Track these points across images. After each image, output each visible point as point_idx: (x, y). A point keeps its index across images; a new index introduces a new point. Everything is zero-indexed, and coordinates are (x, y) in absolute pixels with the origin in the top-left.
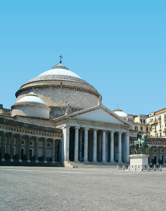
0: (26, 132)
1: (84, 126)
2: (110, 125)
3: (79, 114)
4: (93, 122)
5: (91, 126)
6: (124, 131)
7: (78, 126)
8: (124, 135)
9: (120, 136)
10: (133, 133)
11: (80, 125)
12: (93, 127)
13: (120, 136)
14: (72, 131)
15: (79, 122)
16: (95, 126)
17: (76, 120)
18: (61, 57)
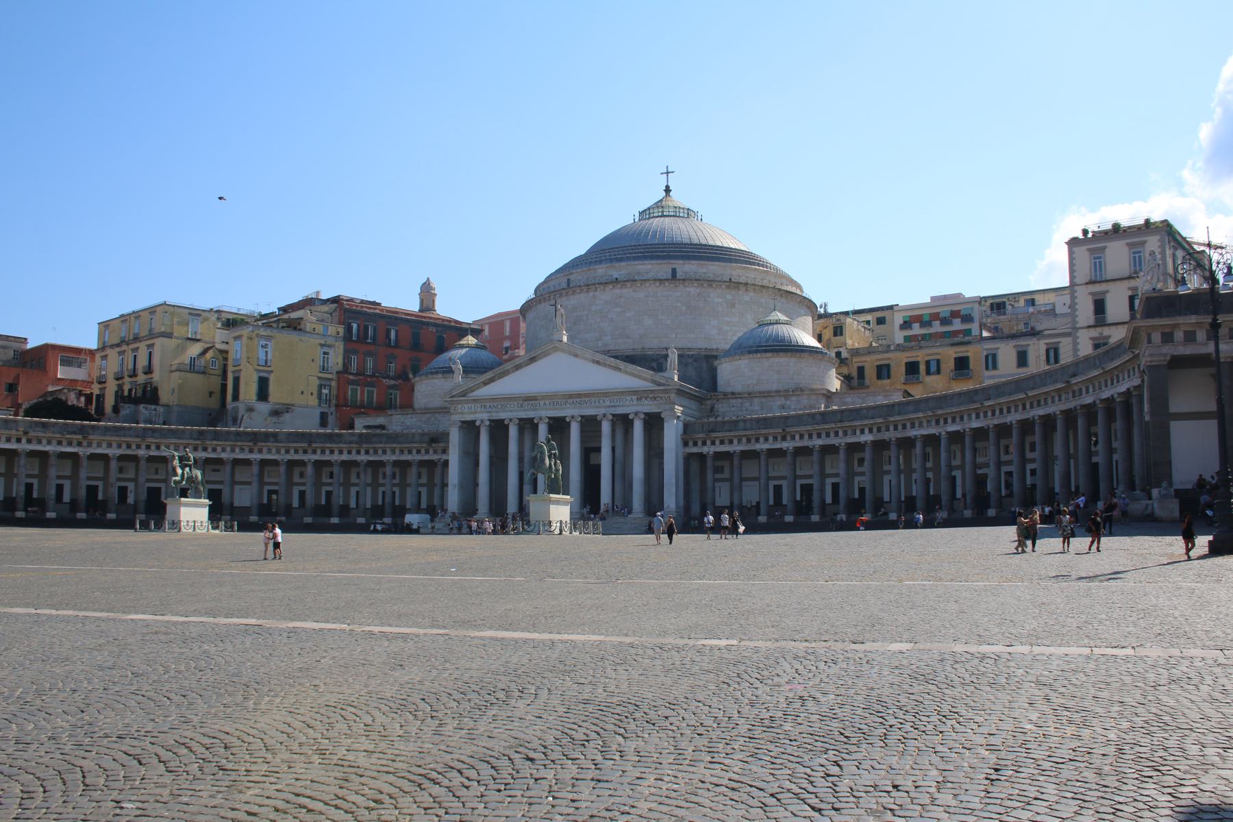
0: (350, 452)
1: (502, 415)
2: (593, 399)
3: (485, 383)
4: (530, 399)
5: (524, 411)
6: (650, 407)
7: (482, 416)
8: (654, 423)
9: (638, 428)
10: (788, 402)
11: (489, 414)
12: (530, 414)
13: (638, 428)
14: (470, 428)
15: (485, 407)
16: (536, 410)
17: (475, 401)
18: (667, 173)
